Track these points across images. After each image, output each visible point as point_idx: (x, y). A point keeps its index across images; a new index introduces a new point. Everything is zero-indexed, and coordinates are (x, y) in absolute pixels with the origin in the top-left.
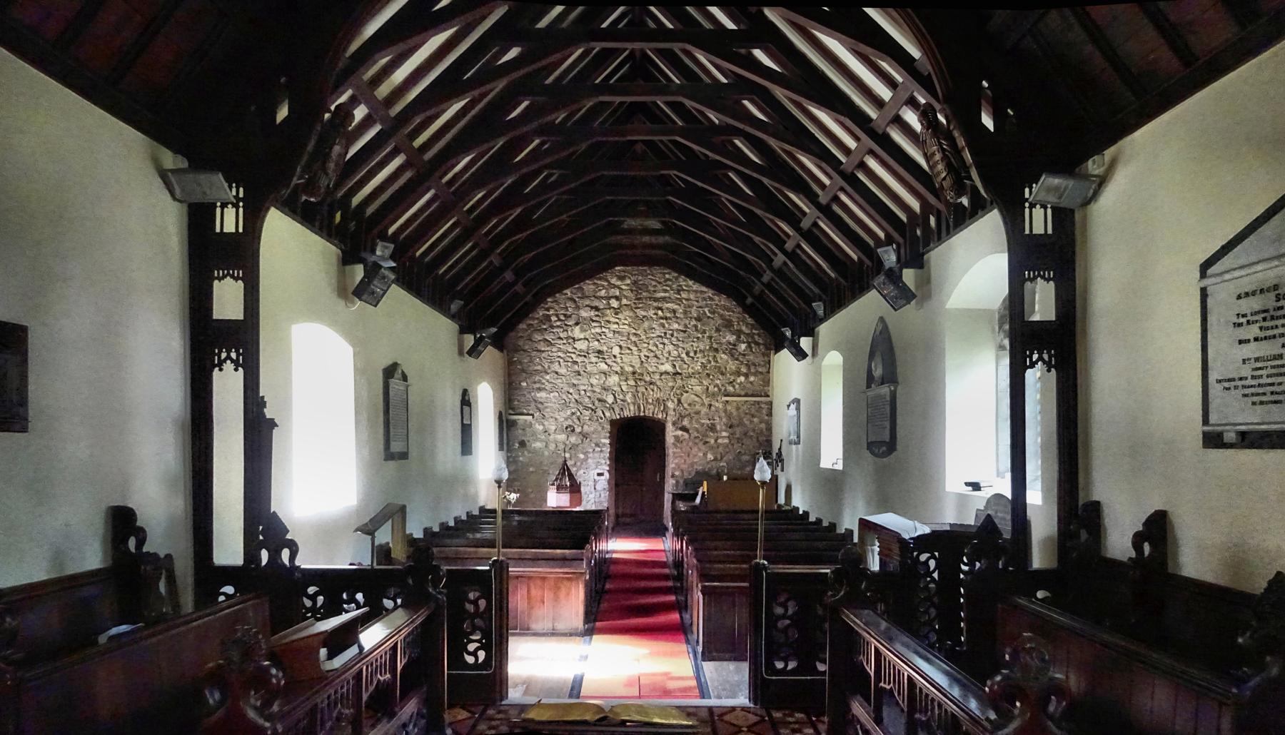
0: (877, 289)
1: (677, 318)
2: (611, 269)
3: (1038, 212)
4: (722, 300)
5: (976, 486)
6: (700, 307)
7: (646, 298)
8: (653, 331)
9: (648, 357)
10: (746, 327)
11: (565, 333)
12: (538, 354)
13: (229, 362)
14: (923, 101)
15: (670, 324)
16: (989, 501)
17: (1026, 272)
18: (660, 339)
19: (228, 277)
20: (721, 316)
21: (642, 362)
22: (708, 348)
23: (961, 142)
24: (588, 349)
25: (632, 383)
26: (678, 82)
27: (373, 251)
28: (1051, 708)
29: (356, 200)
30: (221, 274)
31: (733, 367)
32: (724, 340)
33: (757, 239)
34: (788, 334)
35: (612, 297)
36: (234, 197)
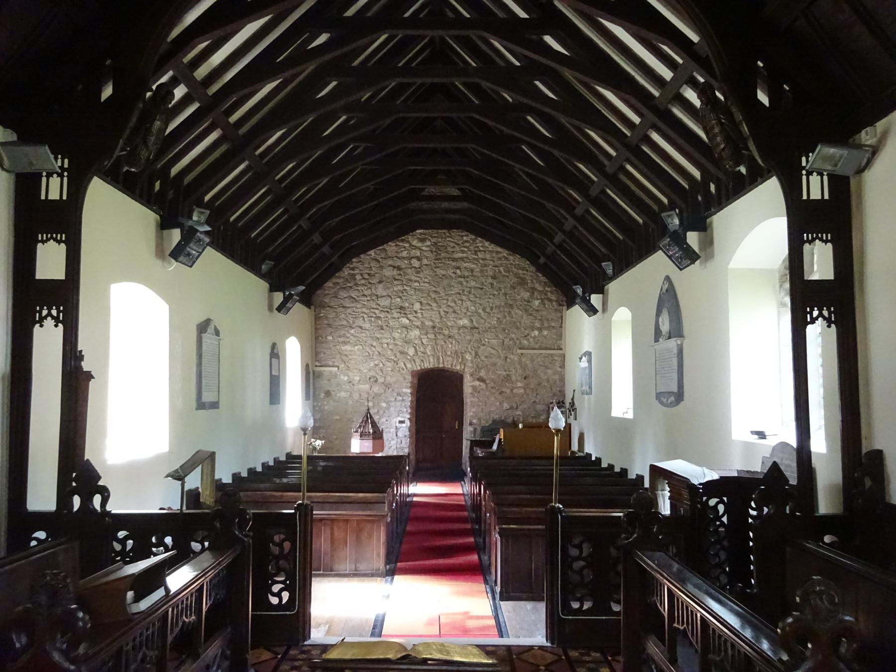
0: (662, 250)
2: (412, 232)
3: (815, 179)
5: (761, 435)
9: (447, 312)
10: (540, 284)
11: (369, 290)
13: (49, 318)
14: (702, 80)
15: (467, 282)
16: (774, 448)
17: (805, 235)
18: (458, 296)
19: (52, 241)
20: (516, 275)
21: (441, 317)
22: (503, 304)
23: (739, 117)
24: (390, 306)
25: (432, 336)
27: (190, 218)
28: (843, 650)
29: (175, 171)
30: (45, 238)
32: (519, 297)
33: (549, 206)
34: (579, 291)
35: (413, 258)
36: (59, 167)
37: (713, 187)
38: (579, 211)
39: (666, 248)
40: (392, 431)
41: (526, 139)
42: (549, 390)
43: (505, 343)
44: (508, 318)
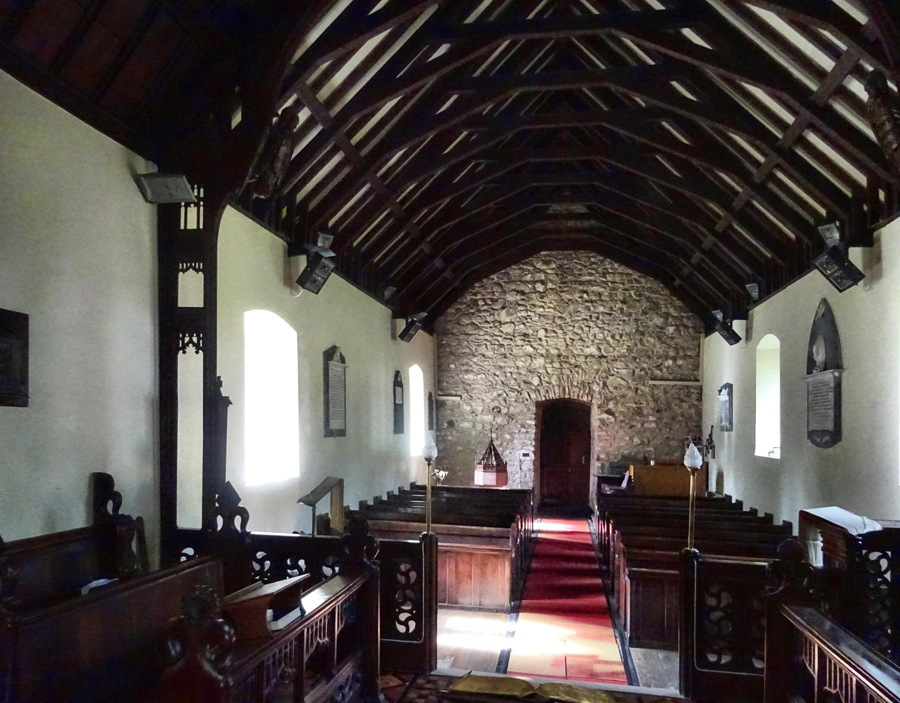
1: (603, 301)
2: (536, 254)
4: (647, 283)
6: (626, 290)
7: (571, 282)
8: (579, 314)
9: (573, 340)
11: (492, 316)
12: (466, 337)
13: (191, 345)
14: (870, 69)
18: (585, 322)
19: (191, 270)
20: (648, 299)
21: (567, 345)
22: (634, 331)
24: (514, 333)
25: (557, 365)
26: (603, 67)
29: (300, 196)
31: (661, 352)
34: (719, 316)
35: (537, 281)
36: (196, 196)
37: (882, 195)
38: (720, 227)
39: (822, 267)
40: (515, 464)
41: (662, 148)
42: (684, 424)
43: (636, 372)
44: (639, 346)
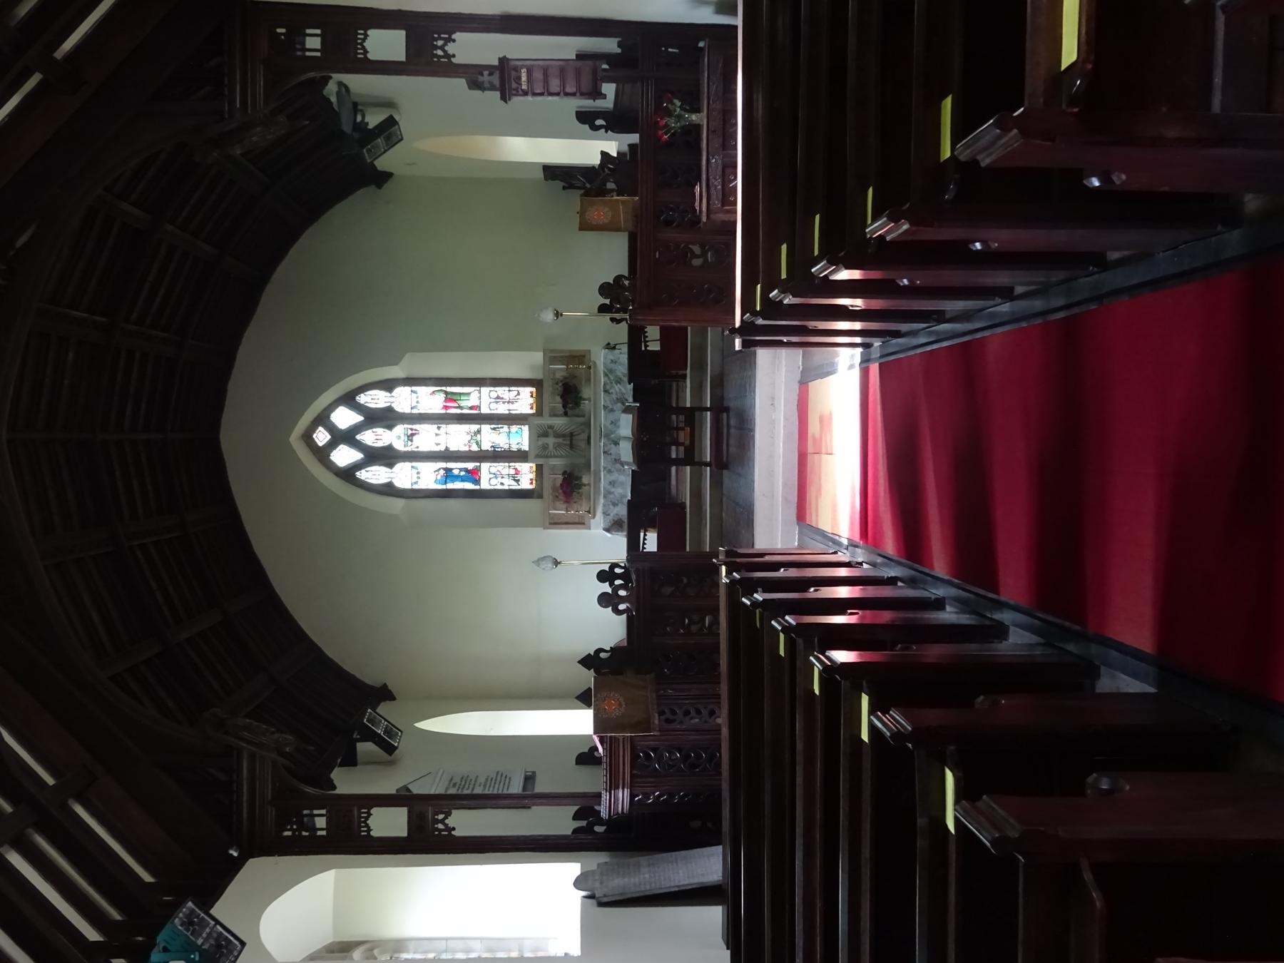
13: (446, 48)
30: (362, 51)
